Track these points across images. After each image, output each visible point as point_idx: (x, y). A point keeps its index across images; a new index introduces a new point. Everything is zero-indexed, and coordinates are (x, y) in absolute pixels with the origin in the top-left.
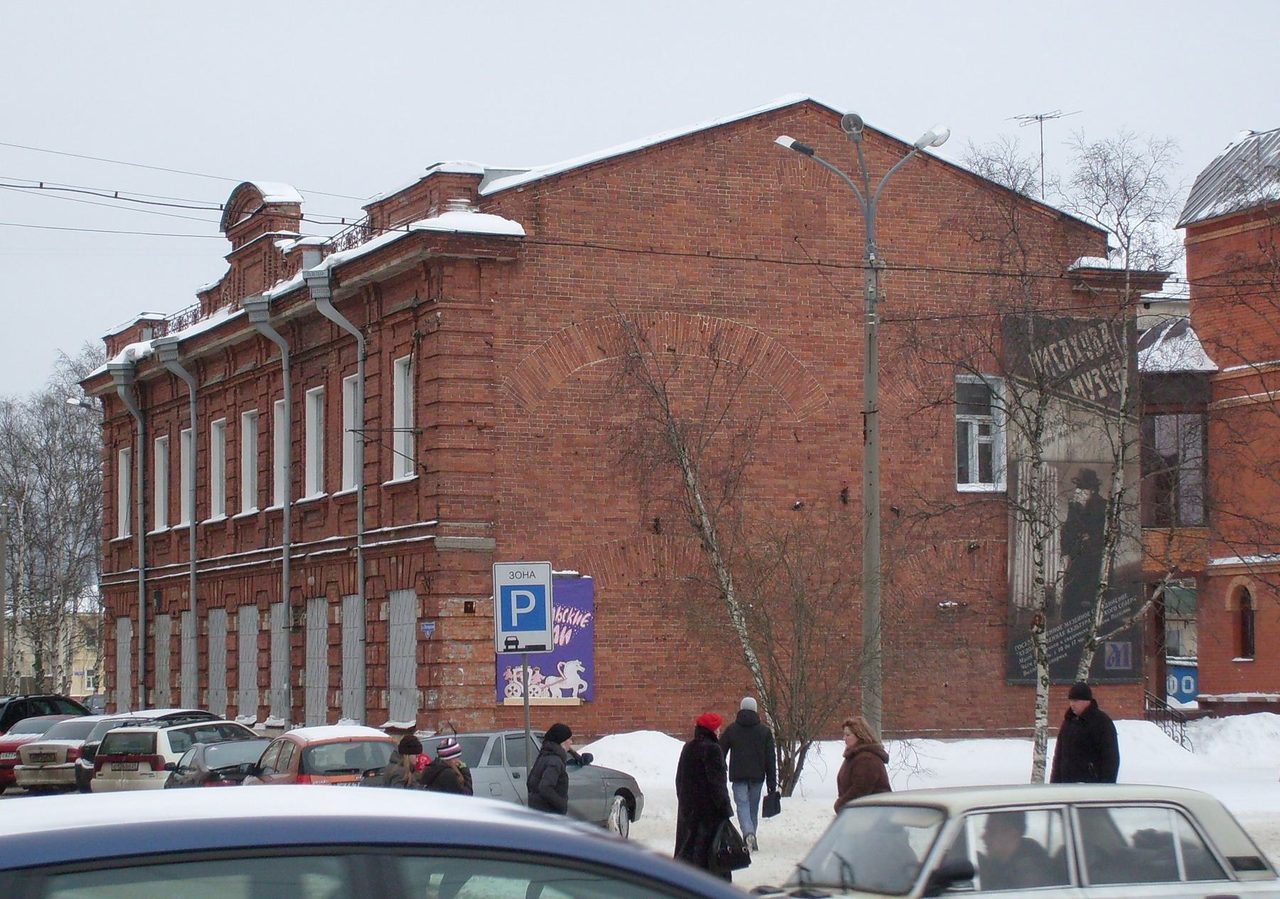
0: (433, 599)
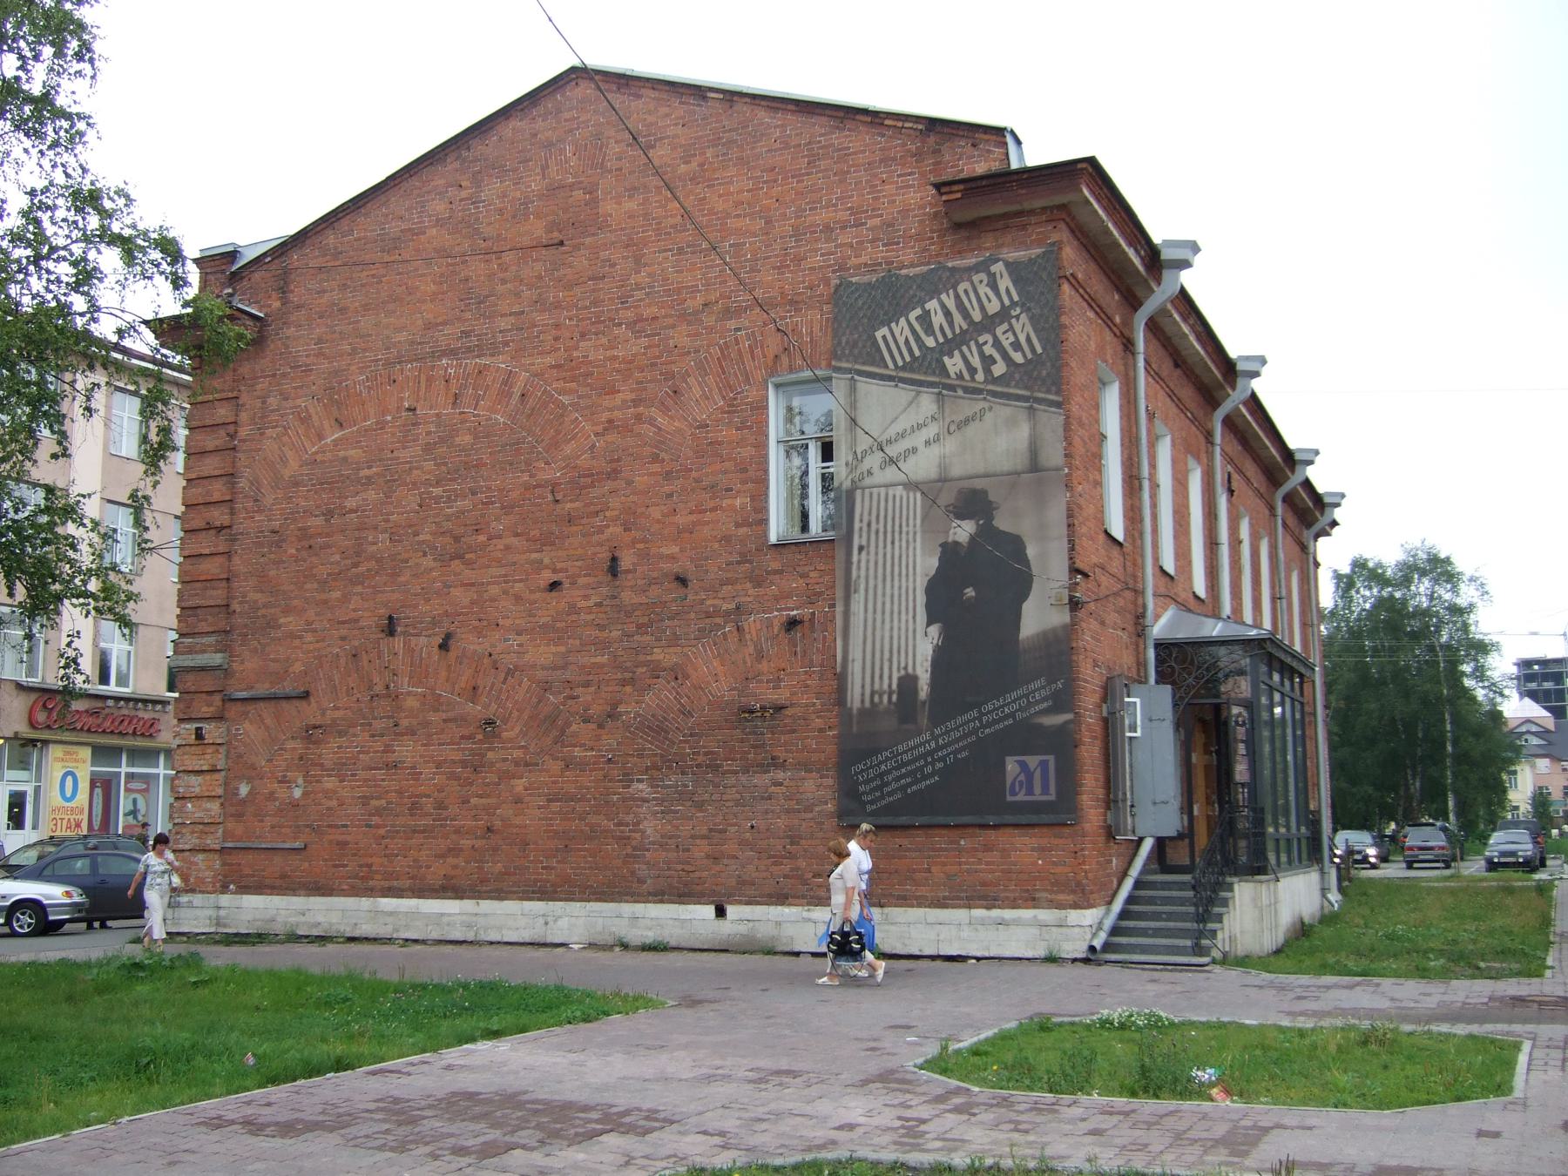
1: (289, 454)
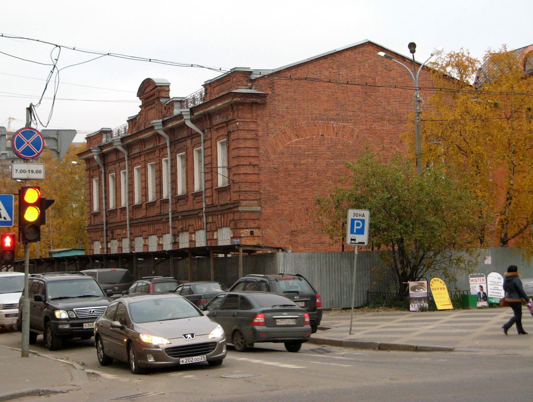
0: (238, 230)
1: (279, 144)
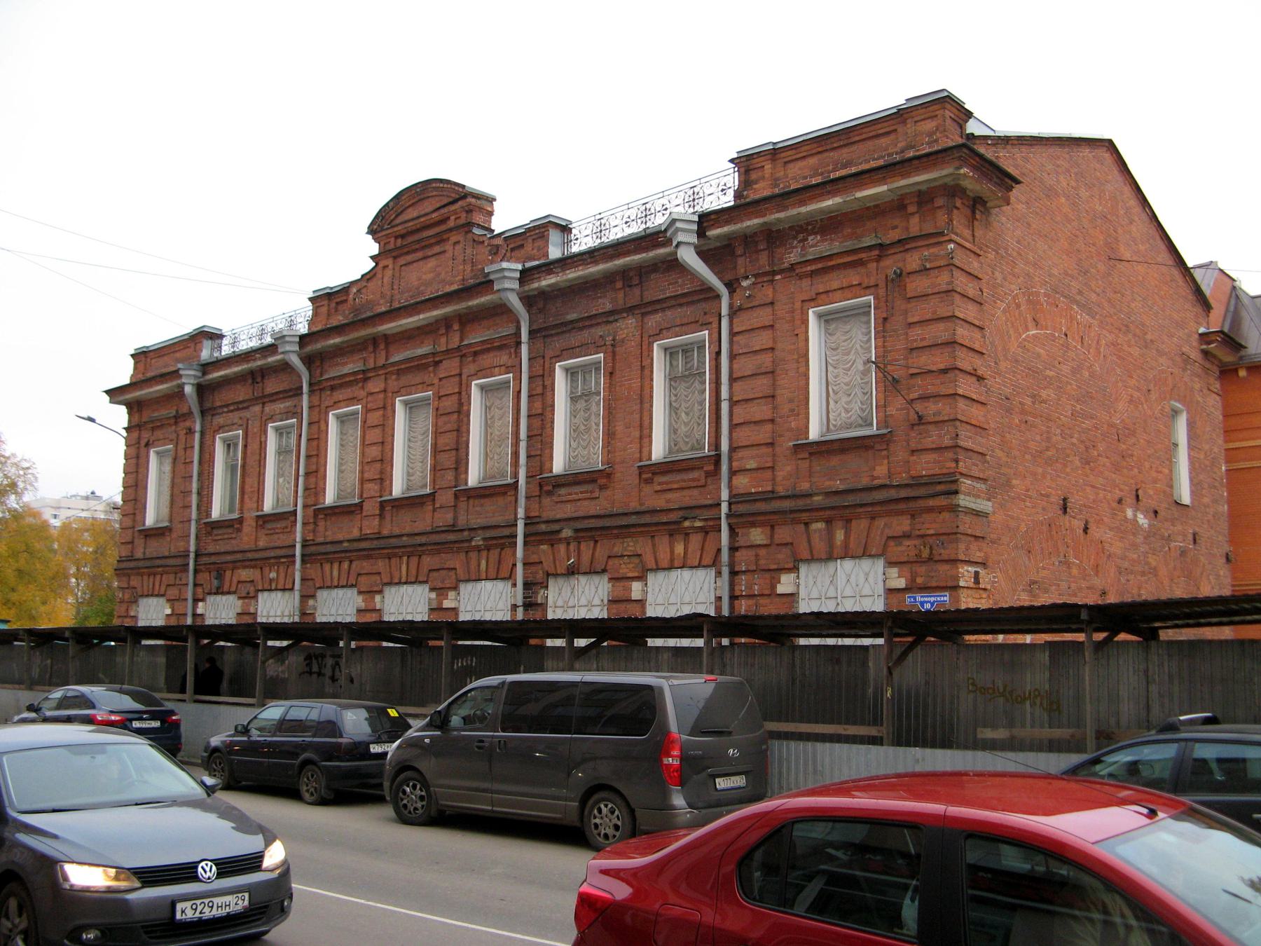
1: (1011, 332)
